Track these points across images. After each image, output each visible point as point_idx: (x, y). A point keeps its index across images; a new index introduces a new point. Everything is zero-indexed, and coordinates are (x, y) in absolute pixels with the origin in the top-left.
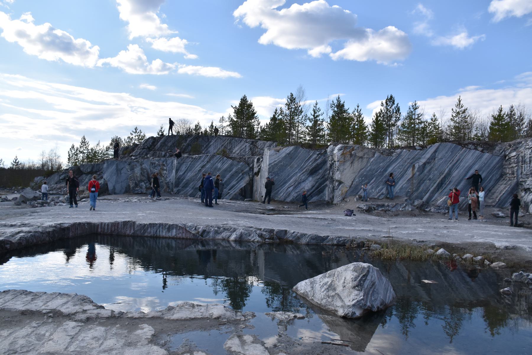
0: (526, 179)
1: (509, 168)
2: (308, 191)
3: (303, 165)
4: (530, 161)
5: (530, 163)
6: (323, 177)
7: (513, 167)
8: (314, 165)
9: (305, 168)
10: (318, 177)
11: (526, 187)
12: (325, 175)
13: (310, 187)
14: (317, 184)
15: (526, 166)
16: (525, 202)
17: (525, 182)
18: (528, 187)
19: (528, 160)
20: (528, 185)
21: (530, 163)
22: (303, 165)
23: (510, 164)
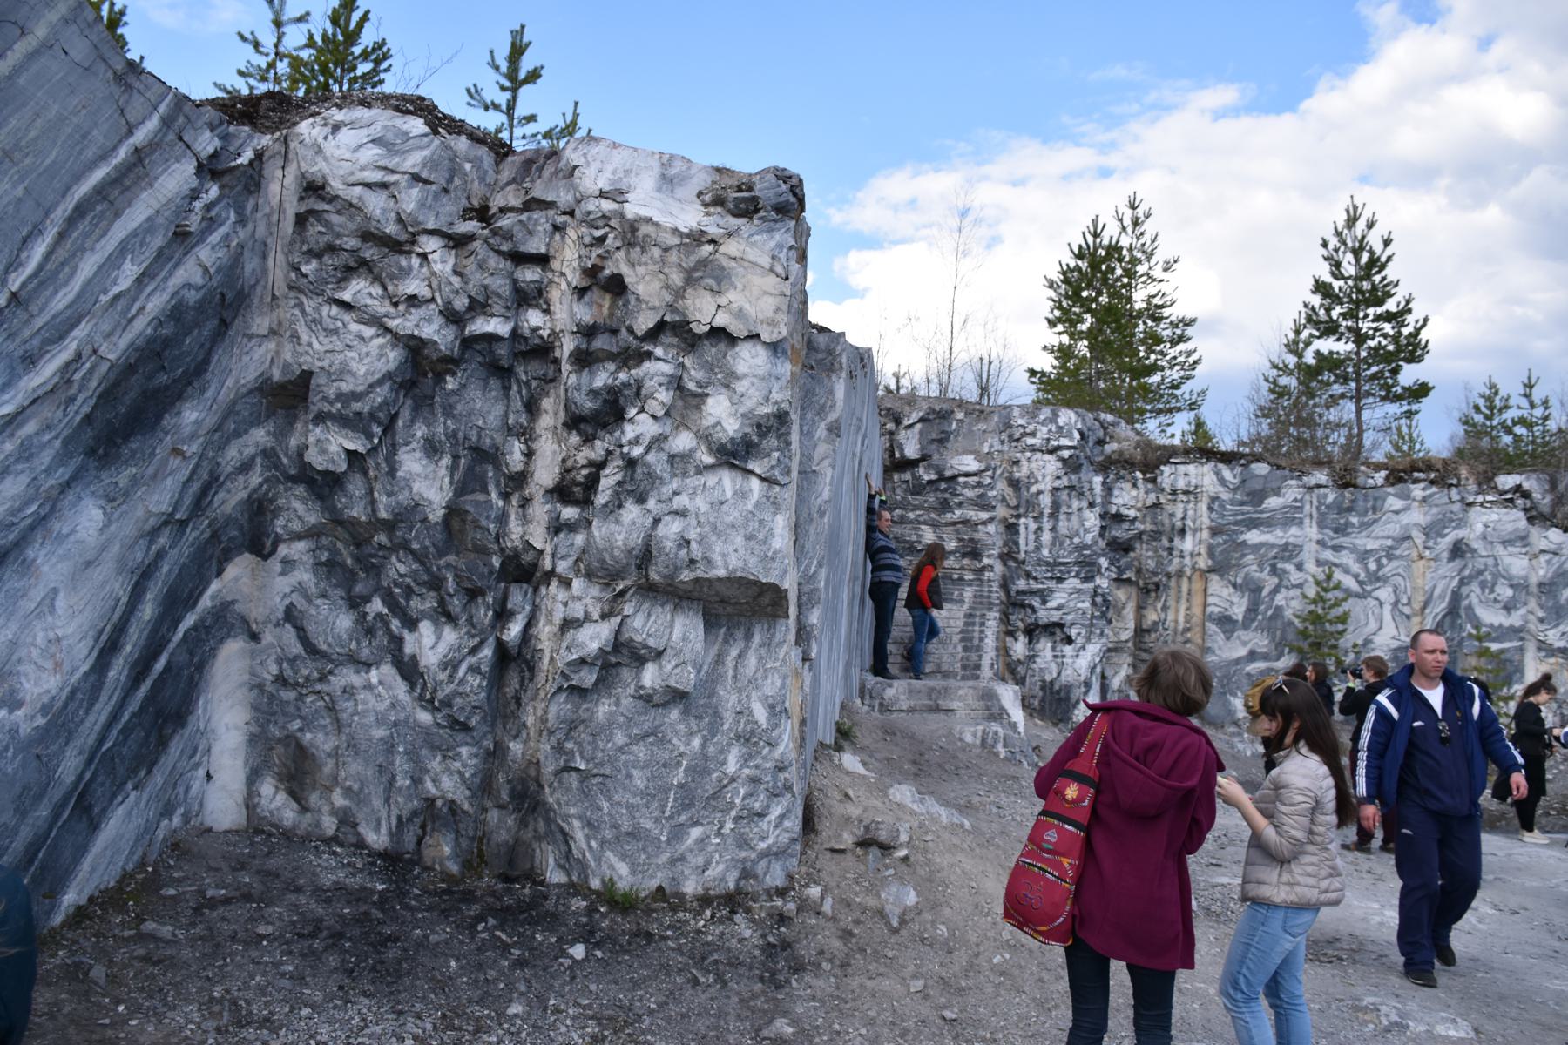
0: (1052, 584)
1: (935, 525)
2: (59, 722)
3: (46, 278)
4: (1056, 506)
5: (1054, 515)
6: (200, 505)
7: (965, 522)
8: (156, 303)
9: (60, 331)
10: (160, 499)
11: (1045, 615)
12: (213, 483)
13: (81, 656)
14: (148, 611)
15: (1033, 526)
16: (1047, 687)
17: (1044, 596)
18: (1056, 616)
19: (1046, 500)
20: (1058, 608)
21: (1054, 515)
22: (46, 278)
23: (945, 506)
